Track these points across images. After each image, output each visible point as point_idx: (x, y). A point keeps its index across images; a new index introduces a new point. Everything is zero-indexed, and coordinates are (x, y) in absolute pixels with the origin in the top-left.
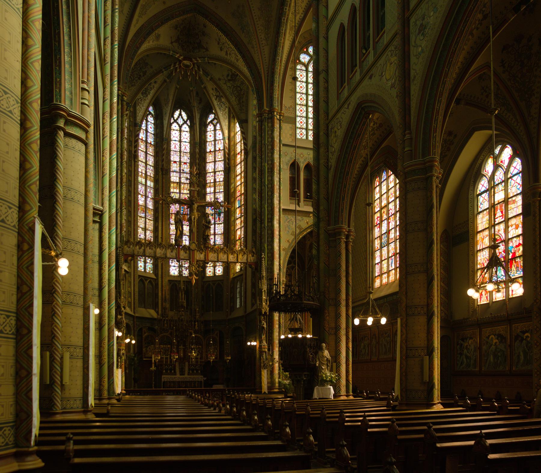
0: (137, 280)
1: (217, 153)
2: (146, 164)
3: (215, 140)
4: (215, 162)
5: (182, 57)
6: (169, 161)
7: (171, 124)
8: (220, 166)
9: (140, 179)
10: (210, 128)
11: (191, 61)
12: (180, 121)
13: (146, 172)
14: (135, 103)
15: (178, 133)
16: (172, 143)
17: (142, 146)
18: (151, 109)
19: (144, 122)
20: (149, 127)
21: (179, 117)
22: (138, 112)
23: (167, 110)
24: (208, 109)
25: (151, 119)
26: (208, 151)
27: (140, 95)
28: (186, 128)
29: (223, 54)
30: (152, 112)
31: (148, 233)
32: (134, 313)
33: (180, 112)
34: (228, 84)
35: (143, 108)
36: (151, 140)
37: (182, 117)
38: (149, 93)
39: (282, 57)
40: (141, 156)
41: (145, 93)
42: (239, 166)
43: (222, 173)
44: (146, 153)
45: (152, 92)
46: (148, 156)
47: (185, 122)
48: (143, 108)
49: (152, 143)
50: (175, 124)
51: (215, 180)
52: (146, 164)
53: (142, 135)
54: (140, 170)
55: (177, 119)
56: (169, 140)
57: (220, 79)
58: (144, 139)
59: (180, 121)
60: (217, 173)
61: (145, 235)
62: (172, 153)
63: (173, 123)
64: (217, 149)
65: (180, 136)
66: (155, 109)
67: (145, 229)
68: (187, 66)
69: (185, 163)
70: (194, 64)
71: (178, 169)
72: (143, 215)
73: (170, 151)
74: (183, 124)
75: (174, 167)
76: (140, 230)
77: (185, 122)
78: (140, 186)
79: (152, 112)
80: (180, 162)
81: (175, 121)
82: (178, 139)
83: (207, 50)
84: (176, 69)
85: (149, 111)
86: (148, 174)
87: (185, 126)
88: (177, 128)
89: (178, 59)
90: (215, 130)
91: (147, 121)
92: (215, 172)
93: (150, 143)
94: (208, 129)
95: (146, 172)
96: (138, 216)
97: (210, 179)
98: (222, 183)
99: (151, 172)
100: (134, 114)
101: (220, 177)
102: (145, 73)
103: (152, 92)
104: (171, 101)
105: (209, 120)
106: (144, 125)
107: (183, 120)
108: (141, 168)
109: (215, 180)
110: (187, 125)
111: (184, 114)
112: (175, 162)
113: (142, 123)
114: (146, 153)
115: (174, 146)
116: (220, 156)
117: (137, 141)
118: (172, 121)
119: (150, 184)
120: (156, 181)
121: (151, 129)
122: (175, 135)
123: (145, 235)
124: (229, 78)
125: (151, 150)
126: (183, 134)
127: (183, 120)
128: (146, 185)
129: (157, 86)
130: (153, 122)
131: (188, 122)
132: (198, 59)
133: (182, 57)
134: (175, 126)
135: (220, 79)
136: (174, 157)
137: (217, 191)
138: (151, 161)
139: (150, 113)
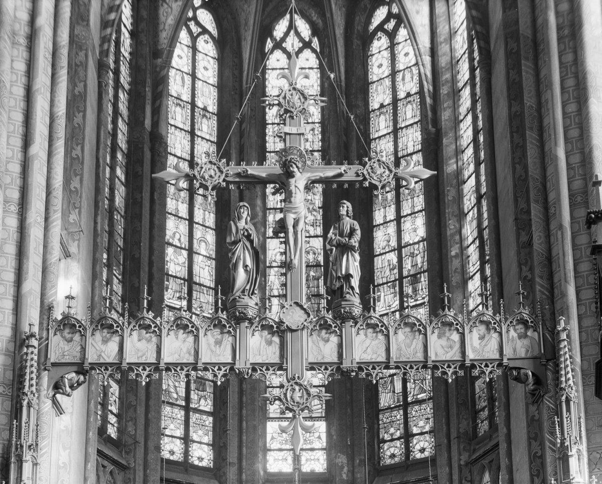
3: (394, 74)
4: (396, 131)
10: (380, 44)
12: (292, 43)
20: (200, 65)
21: (287, 34)
37: (298, 34)
49: (210, 109)
55: (283, 39)
58: (186, 97)
59: (292, 43)
63: (272, 52)
64: (401, 95)
74: (300, 51)
77: (307, 45)
81: (278, 45)
90: (392, 47)
93: (205, 109)
107: (301, 39)
110: (314, 51)
116: (410, 113)
118: (269, 44)
121: (208, 70)
127: (301, 39)
128: (191, 221)
131: (316, 43)
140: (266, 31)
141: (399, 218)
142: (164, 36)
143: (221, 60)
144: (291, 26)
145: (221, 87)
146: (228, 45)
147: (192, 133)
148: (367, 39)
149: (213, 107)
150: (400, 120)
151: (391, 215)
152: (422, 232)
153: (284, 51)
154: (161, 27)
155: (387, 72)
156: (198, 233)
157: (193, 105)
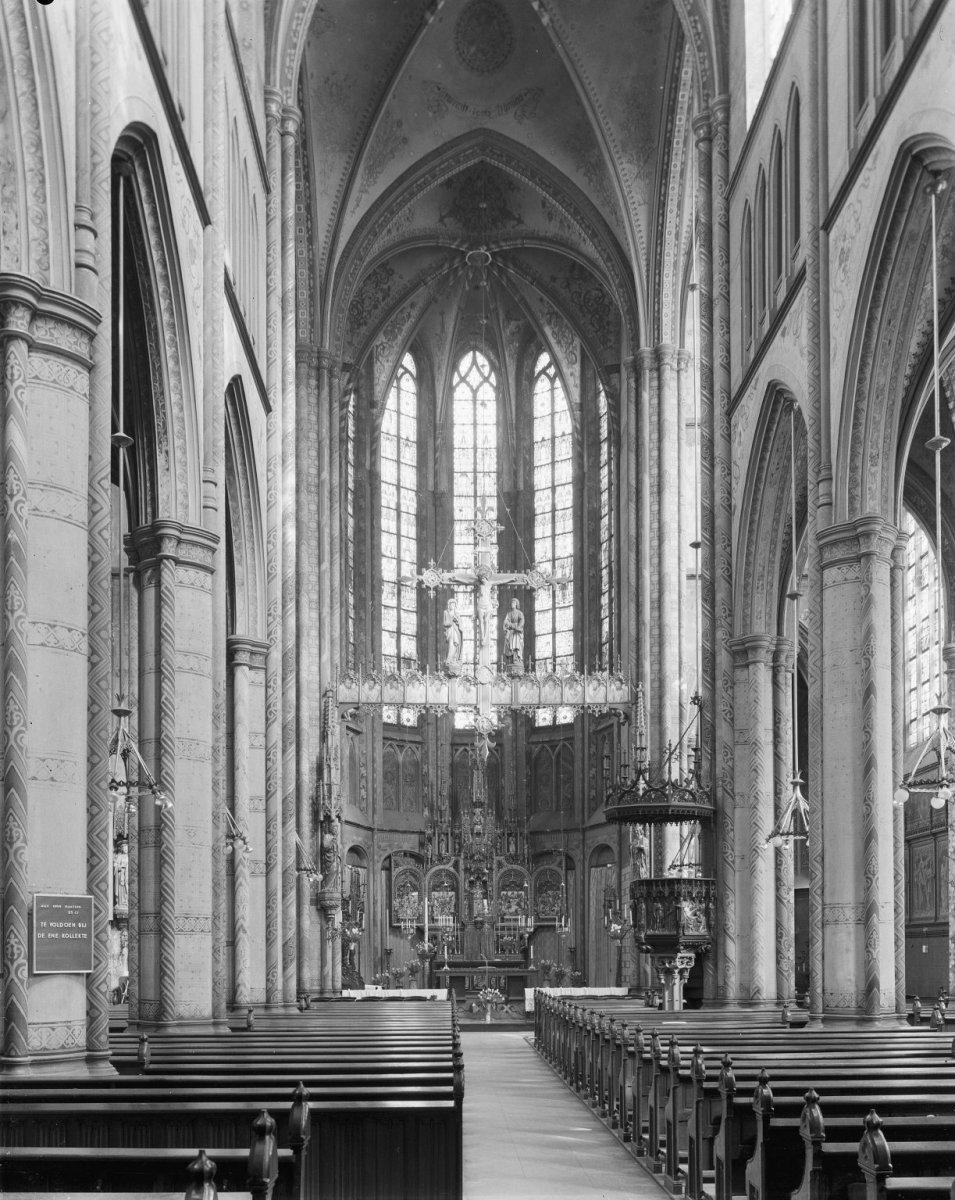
5: (465, 246)
7: (450, 389)
10: (542, 386)
12: (475, 378)
14: (371, 357)
18: (408, 361)
19: (393, 391)
22: (377, 374)
23: (442, 359)
24: (530, 343)
27: (381, 338)
33: (474, 354)
35: (386, 365)
38: (400, 330)
41: (392, 331)
46: (403, 467)
48: (386, 365)
51: (554, 505)
55: (467, 375)
56: (448, 424)
57: (554, 279)
59: (475, 378)
60: (559, 489)
63: (458, 384)
64: (558, 433)
66: (417, 361)
70: (494, 255)
74: (481, 384)
77: (486, 379)
80: (475, 471)
81: (463, 379)
83: (520, 221)
85: (402, 367)
88: (469, 395)
89: (457, 250)
92: (553, 488)
93: (407, 440)
96: (380, 605)
104: (450, 336)
105: (538, 369)
106: (391, 403)
109: (554, 505)
110: (491, 385)
111: (481, 359)
112: (464, 473)
115: (461, 435)
118: (456, 379)
127: (482, 374)
128: (399, 535)
129: (415, 313)
131: (493, 379)
132: (503, 244)
133: (465, 246)
134: (461, 393)
137: (558, 532)
138: (410, 478)
139: (407, 371)
140: (454, 367)
141: (554, 536)
142: (378, 389)
143: (419, 396)
144: (474, 362)
145: (420, 419)
146: (425, 381)
147: (398, 462)
148: (532, 380)
149: (413, 437)
150: (557, 454)
151: (549, 532)
153: (468, 384)
154: (376, 381)
155: (549, 411)
156: (404, 542)
157: (399, 438)
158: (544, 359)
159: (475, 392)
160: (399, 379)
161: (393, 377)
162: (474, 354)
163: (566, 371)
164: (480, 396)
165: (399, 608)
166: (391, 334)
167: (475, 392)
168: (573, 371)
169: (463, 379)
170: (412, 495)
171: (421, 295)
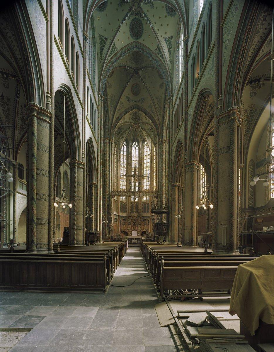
0: (120, 203)
1: (148, 156)
2: (123, 162)
6: (131, 160)
7: (132, 147)
8: (149, 160)
9: (121, 168)
10: (146, 147)
11: (137, 125)
12: (135, 146)
13: (123, 165)
15: (134, 150)
16: (132, 154)
17: (122, 157)
18: (125, 143)
20: (124, 149)
23: (130, 143)
24: (144, 141)
25: (125, 147)
26: (145, 155)
28: (137, 148)
29: (147, 121)
30: (125, 144)
31: (124, 186)
32: (119, 214)
33: (135, 142)
34: (150, 131)
36: (125, 154)
39: (166, 120)
40: (122, 160)
42: (155, 160)
43: (149, 163)
44: (123, 159)
45: (124, 137)
46: (124, 159)
47: (137, 146)
50: (133, 147)
52: (123, 162)
53: (122, 153)
54: (121, 165)
59: (135, 146)
61: (123, 187)
62: (132, 157)
65: (135, 152)
66: (126, 143)
67: (123, 185)
68: (136, 127)
69: (137, 161)
71: (134, 163)
72: (122, 180)
73: (132, 157)
75: (133, 162)
76: (121, 186)
77: (137, 146)
78: (121, 170)
79: (125, 144)
81: (134, 146)
82: (134, 152)
83: (142, 120)
84: (132, 128)
85: (124, 144)
86: (124, 166)
87: (137, 147)
88: (134, 148)
91: (124, 147)
94: (145, 148)
95: (123, 165)
96: (120, 181)
97: (145, 165)
98: (149, 167)
99: (125, 165)
100: (119, 146)
101: (149, 165)
102: (121, 131)
103: (124, 137)
106: (122, 149)
108: (121, 164)
111: (136, 143)
112: (133, 161)
113: (121, 148)
114: (123, 159)
115: (133, 155)
116: (149, 157)
117: (120, 155)
118: (132, 146)
119: (125, 169)
120: (127, 168)
121: (125, 150)
122: (133, 151)
123: (123, 187)
124: (150, 129)
125: (125, 158)
126: (136, 150)
128: (123, 170)
129: (126, 135)
130: (126, 147)
131: (138, 146)
134: (133, 148)
135: (147, 130)
136: (133, 159)
138: (125, 161)
140: (132, 144)
141: (147, 170)
142: (120, 147)
144: (135, 143)
146: (127, 146)
152: (149, 172)
157: (123, 154)
158: (146, 143)
159: (135, 148)
160: (123, 146)
161: (123, 145)
162: (135, 142)
163: (149, 145)
164: (136, 148)
165: (123, 181)
166: (122, 138)
167: (135, 148)
168: (150, 145)
169: (134, 146)
170: (125, 164)
171: (127, 132)
